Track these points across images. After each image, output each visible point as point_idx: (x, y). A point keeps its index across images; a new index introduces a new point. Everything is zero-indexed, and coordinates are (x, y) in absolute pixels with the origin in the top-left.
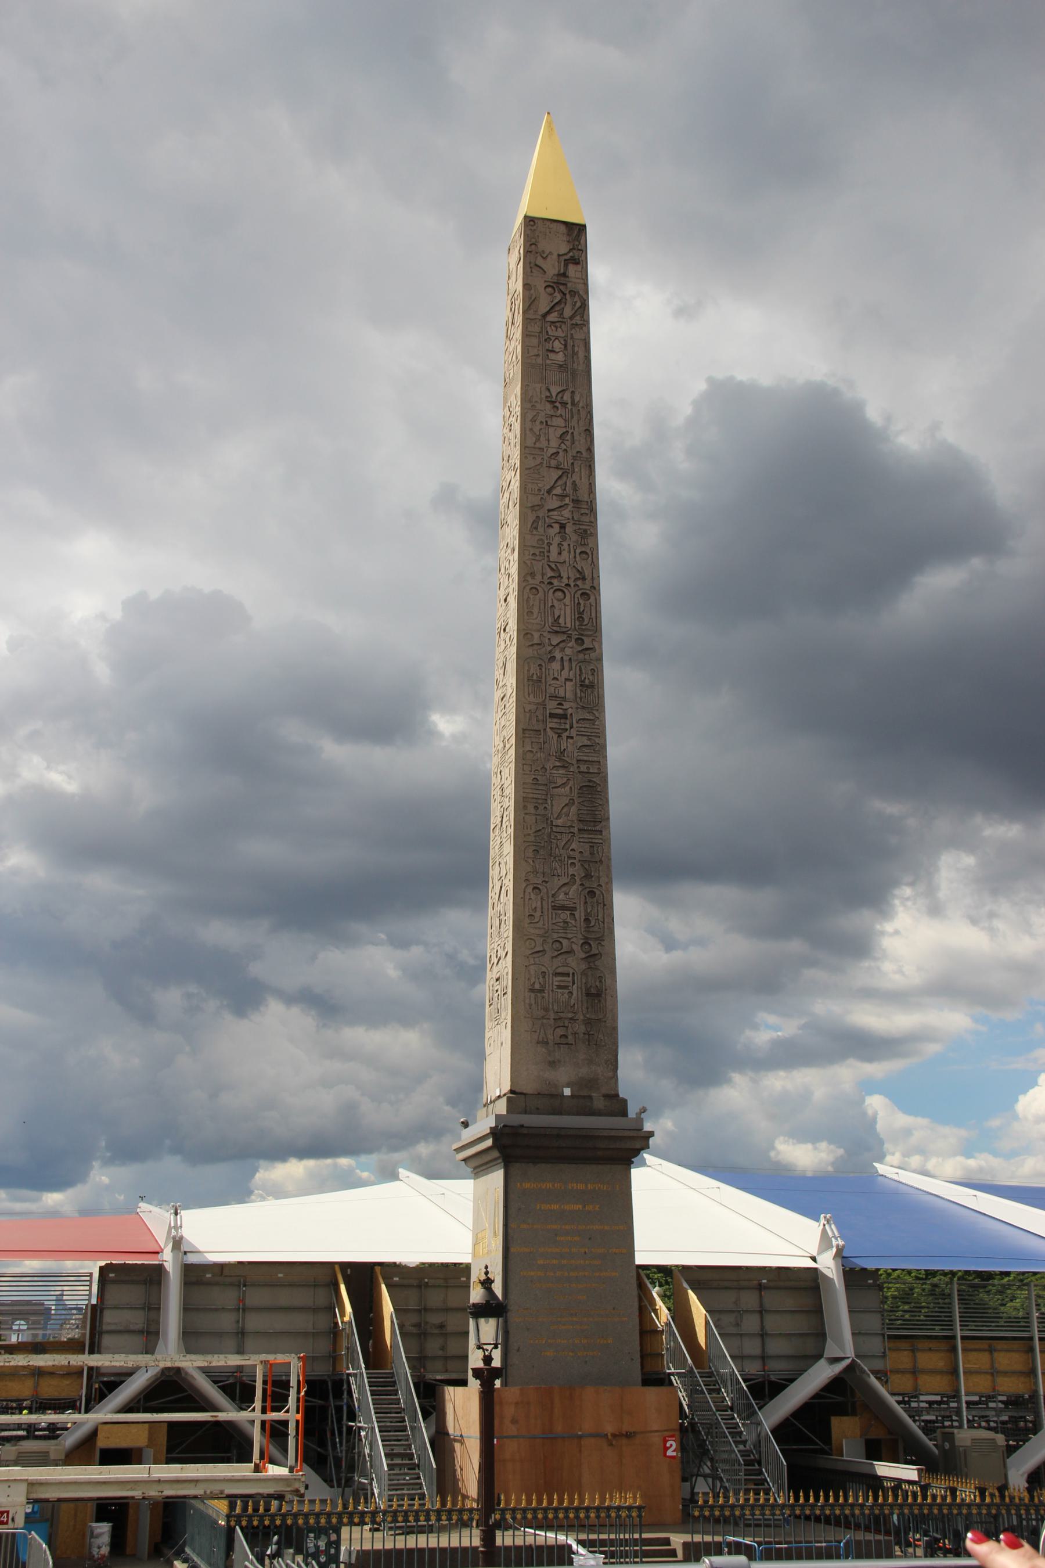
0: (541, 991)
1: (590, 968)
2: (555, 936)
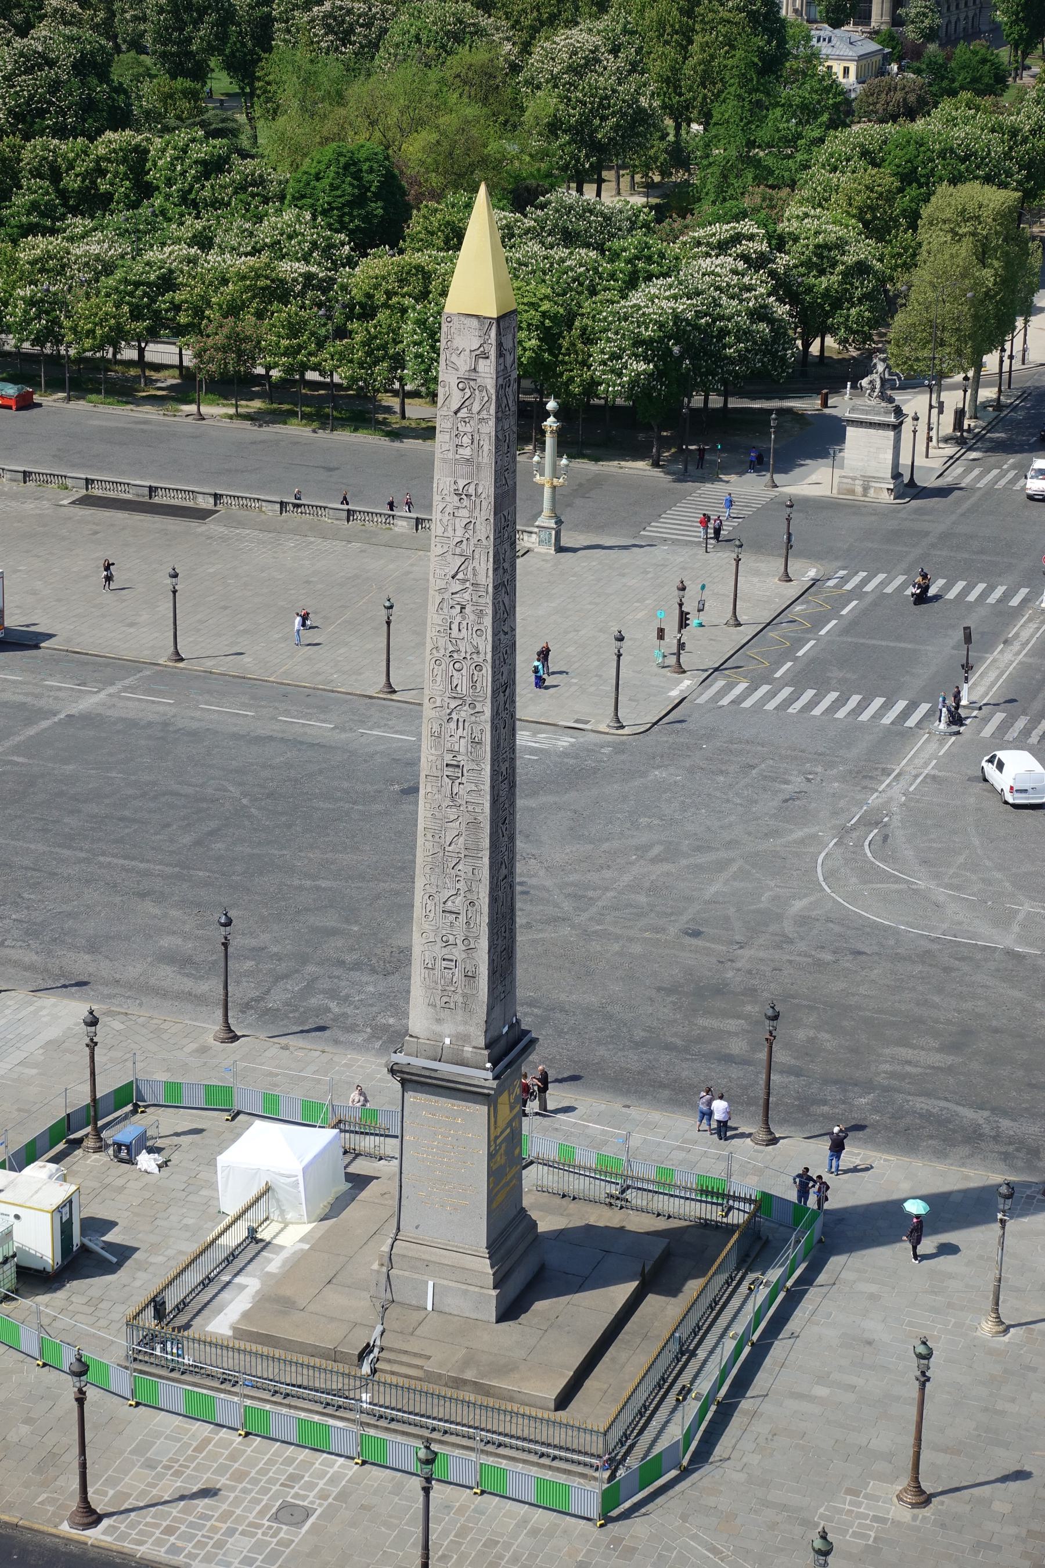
2: (444, 932)
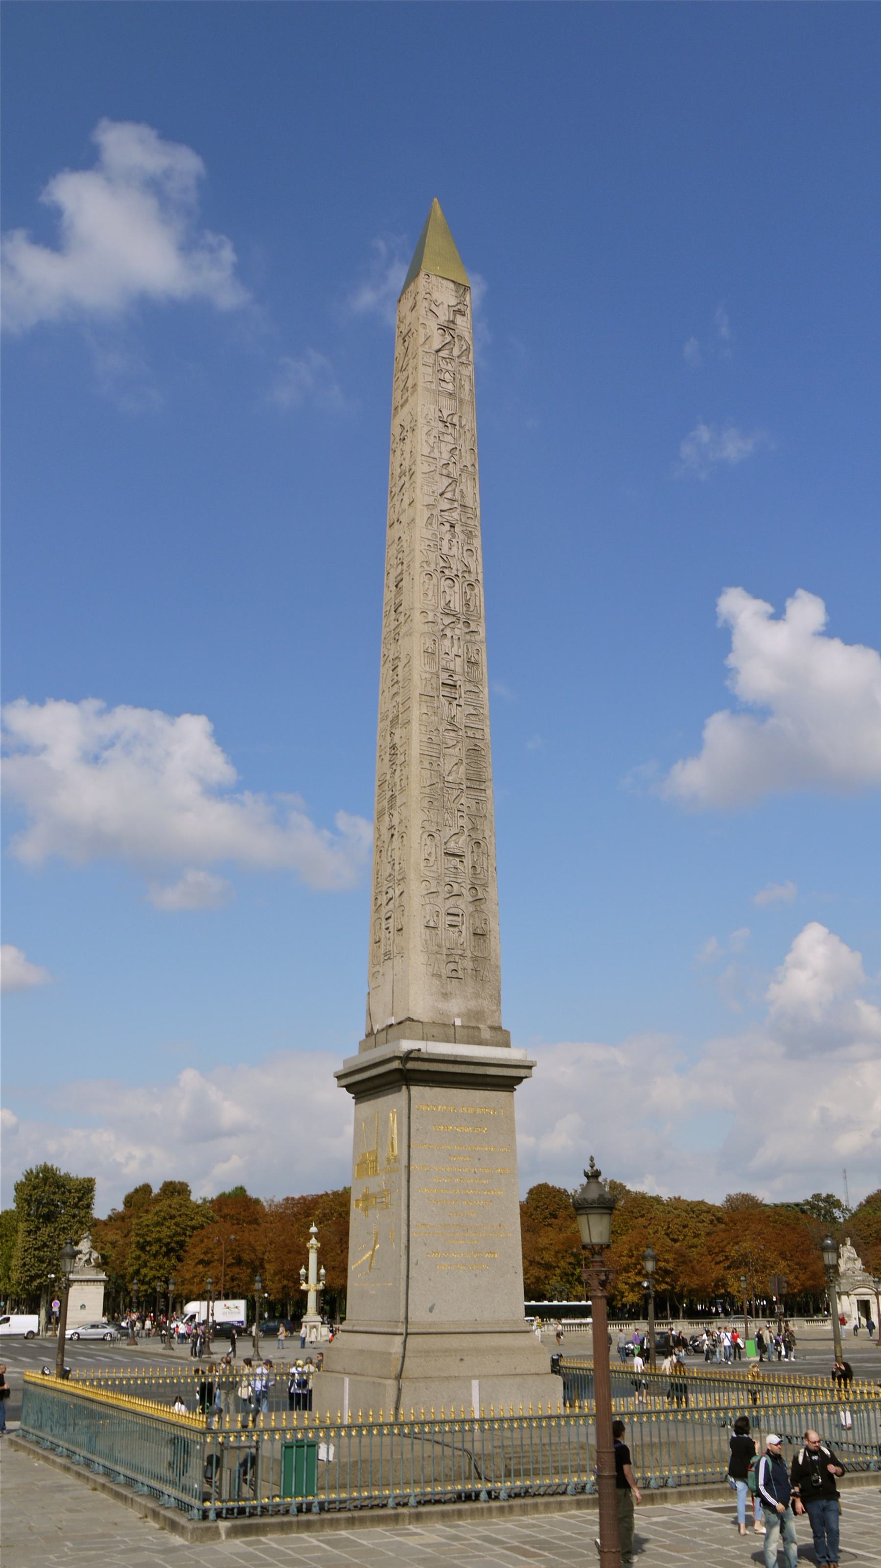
2: (447, 879)
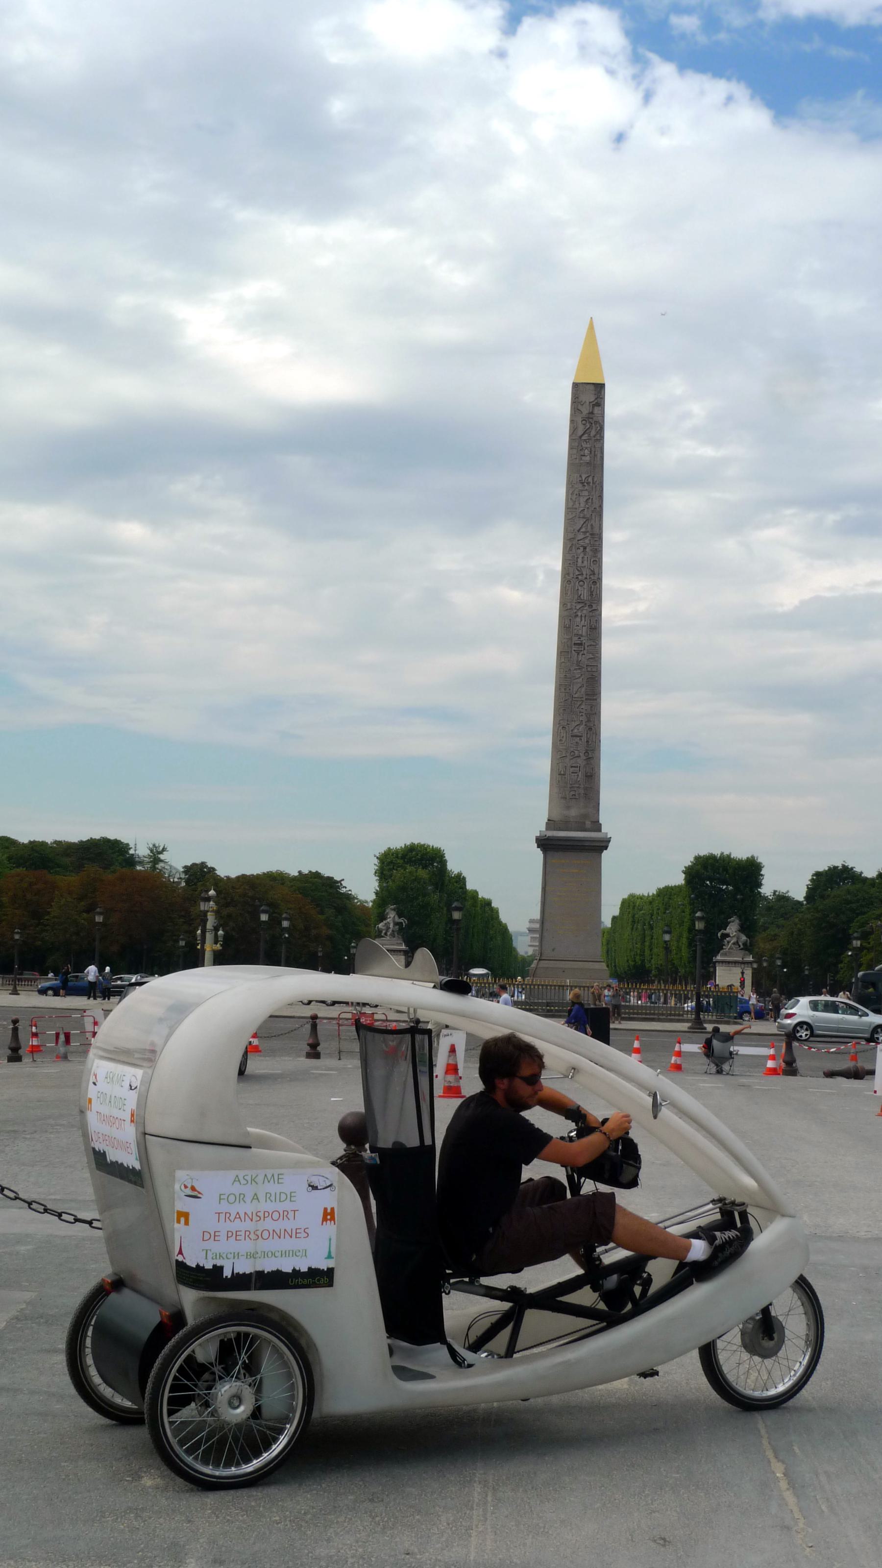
0: (564, 775)
1: (587, 764)
2: (572, 749)
